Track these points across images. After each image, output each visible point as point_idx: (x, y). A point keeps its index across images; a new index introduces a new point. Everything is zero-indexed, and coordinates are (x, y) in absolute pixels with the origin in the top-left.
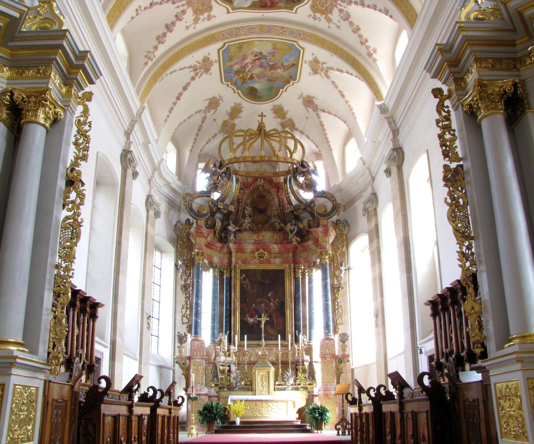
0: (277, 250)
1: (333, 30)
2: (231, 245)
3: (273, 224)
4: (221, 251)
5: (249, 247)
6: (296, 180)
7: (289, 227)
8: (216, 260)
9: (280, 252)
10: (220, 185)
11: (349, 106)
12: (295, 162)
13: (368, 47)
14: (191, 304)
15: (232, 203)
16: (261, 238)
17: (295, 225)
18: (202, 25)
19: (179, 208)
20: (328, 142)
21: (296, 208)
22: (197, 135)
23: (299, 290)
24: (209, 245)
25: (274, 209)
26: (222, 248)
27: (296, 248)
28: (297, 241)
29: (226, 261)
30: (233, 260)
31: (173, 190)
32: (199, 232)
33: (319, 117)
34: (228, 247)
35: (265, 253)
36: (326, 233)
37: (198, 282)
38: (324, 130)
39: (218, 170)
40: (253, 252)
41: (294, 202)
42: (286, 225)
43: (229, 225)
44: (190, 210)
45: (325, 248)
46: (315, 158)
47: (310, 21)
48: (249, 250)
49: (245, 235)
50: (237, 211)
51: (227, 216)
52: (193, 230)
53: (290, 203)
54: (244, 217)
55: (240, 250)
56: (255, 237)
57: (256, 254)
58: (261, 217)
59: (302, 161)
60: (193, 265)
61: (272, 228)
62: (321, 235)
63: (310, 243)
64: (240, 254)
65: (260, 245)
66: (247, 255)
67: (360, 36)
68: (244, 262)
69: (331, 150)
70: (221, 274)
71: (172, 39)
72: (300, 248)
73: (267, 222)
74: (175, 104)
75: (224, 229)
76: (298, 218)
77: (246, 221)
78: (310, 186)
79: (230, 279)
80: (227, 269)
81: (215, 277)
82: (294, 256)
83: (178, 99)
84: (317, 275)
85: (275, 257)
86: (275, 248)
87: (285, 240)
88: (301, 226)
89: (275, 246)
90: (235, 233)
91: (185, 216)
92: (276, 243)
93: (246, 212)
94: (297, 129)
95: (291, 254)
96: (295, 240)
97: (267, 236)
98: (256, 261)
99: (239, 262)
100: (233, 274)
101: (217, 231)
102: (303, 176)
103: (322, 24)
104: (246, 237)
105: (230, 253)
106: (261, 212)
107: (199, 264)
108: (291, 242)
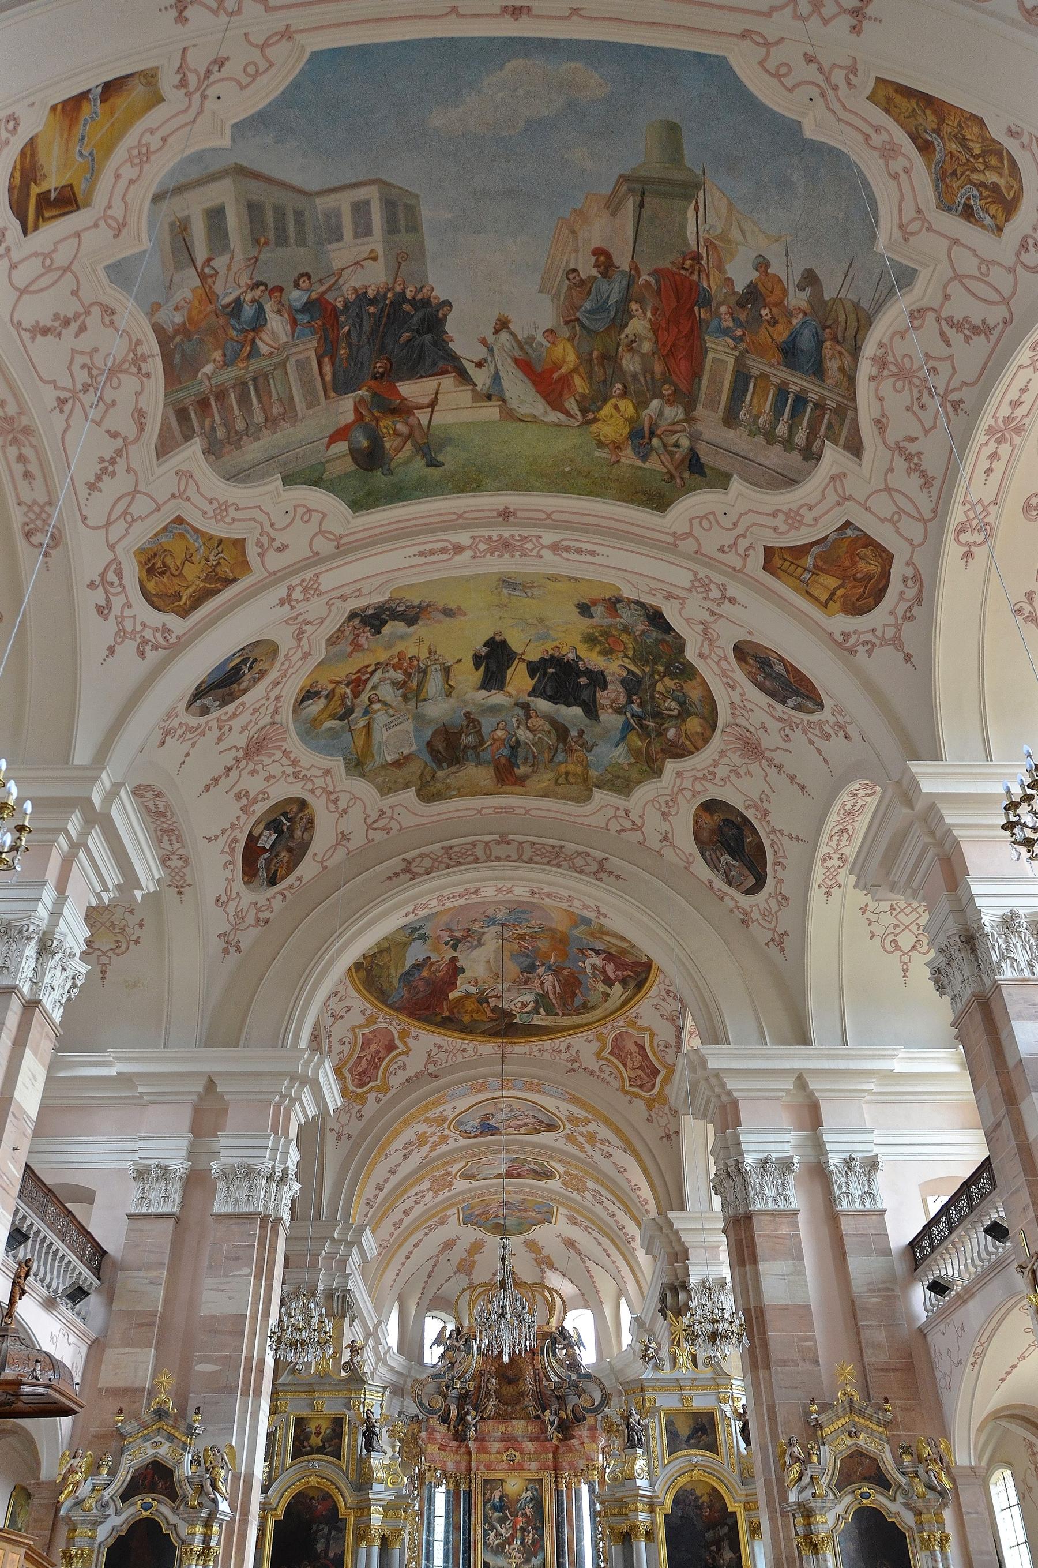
0: (533, 1450)
1: (587, 1203)
2: (471, 1444)
3: (527, 1407)
4: (456, 1452)
5: (495, 1446)
6: (555, 1355)
7: (548, 1416)
8: (450, 1466)
9: (536, 1453)
10: (457, 1364)
11: (617, 1267)
12: (554, 1330)
13: (626, 1234)
14: (420, 1540)
15: (472, 1379)
16: (510, 1429)
17: (556, 1414)
18: (440, 1197)
19: (402, 1390)
20: (597, 1292)
21: (557, 1387)
22: (426, 1282)
23: (562, 1512)
24: (442, 1448)
25: (528, 1385)
26: (459, 1447)
27: (557, 1447)
28: (558, 1438)
29: (463, 1466)
30: (473, 1464)
31: (397, 1372)
32: (431, 1439)
33: (584, 1262)
34: (467, 1446)
35: (516, 1453)
36: (594, 1439)
37: (429, 1509)
38: (592, 1277)
39: (456, 1344)
40: (499, 1453)
41: (554, 1378)
42: (543, 1413)
43: (467, 1413)
44: (421, 1404)
45: (592, 1460)
46: (583, 1303)
47: (563, 1191)
48: (494, 1450)
49: (489, 1425)
50: (478, 1389)
51: (463, 1399)
52: (423, 1434)
53: (549, 1379)
54: (488, 1396)
55: (482, 1450)
56: (502, 1428)
57: (505, 1458)
58: (509, 1391)
59: (563, 1327)
60: (423, 1482)
61: (527, 1418)
62: (586, 1440)
63: (575, 1442)
64: (482, 1456)
65: (508, 1440)
66: (493, 1457)
67: (617, 1222)
68: (488, 1467)
69: (602, 1303)
70: (458, 1484)
71: (407, 1220)
72: (562, 1450)
73: (519, 1402)
74: (403, 1264)
75: (462, 1419)
76: (562, 1399)
77: (491, 1404)
78: (574, 1365)
79: (468, 1494)
80: (465, 1479)
81: (448, 1492)
82: (555, 1457)
83: (408, 1258)
84: (585, 1489)
85: (530, 1460)
86: (530, 1446)
87: (541, 1437)
88: (565, 1416)
89: (530, 1444)
90: (475, 1425)
91: (413, 1409)
92: (531, 1440)
93: (490, 1387)
94: (556, 1269)
95: (551, 1456)
96: (554, 1436)
97: (519, 1427)
98: (506, 1466)
99: (482, 1467)
100: (473, 1486)
101: (452, 1423)
102: (563, 1349)
103: (575, 1195)
104: (491, 1429)
105: (469, 1453)
106: (512, 1381)
107: (430, 1483)
108: (551, 1440)
